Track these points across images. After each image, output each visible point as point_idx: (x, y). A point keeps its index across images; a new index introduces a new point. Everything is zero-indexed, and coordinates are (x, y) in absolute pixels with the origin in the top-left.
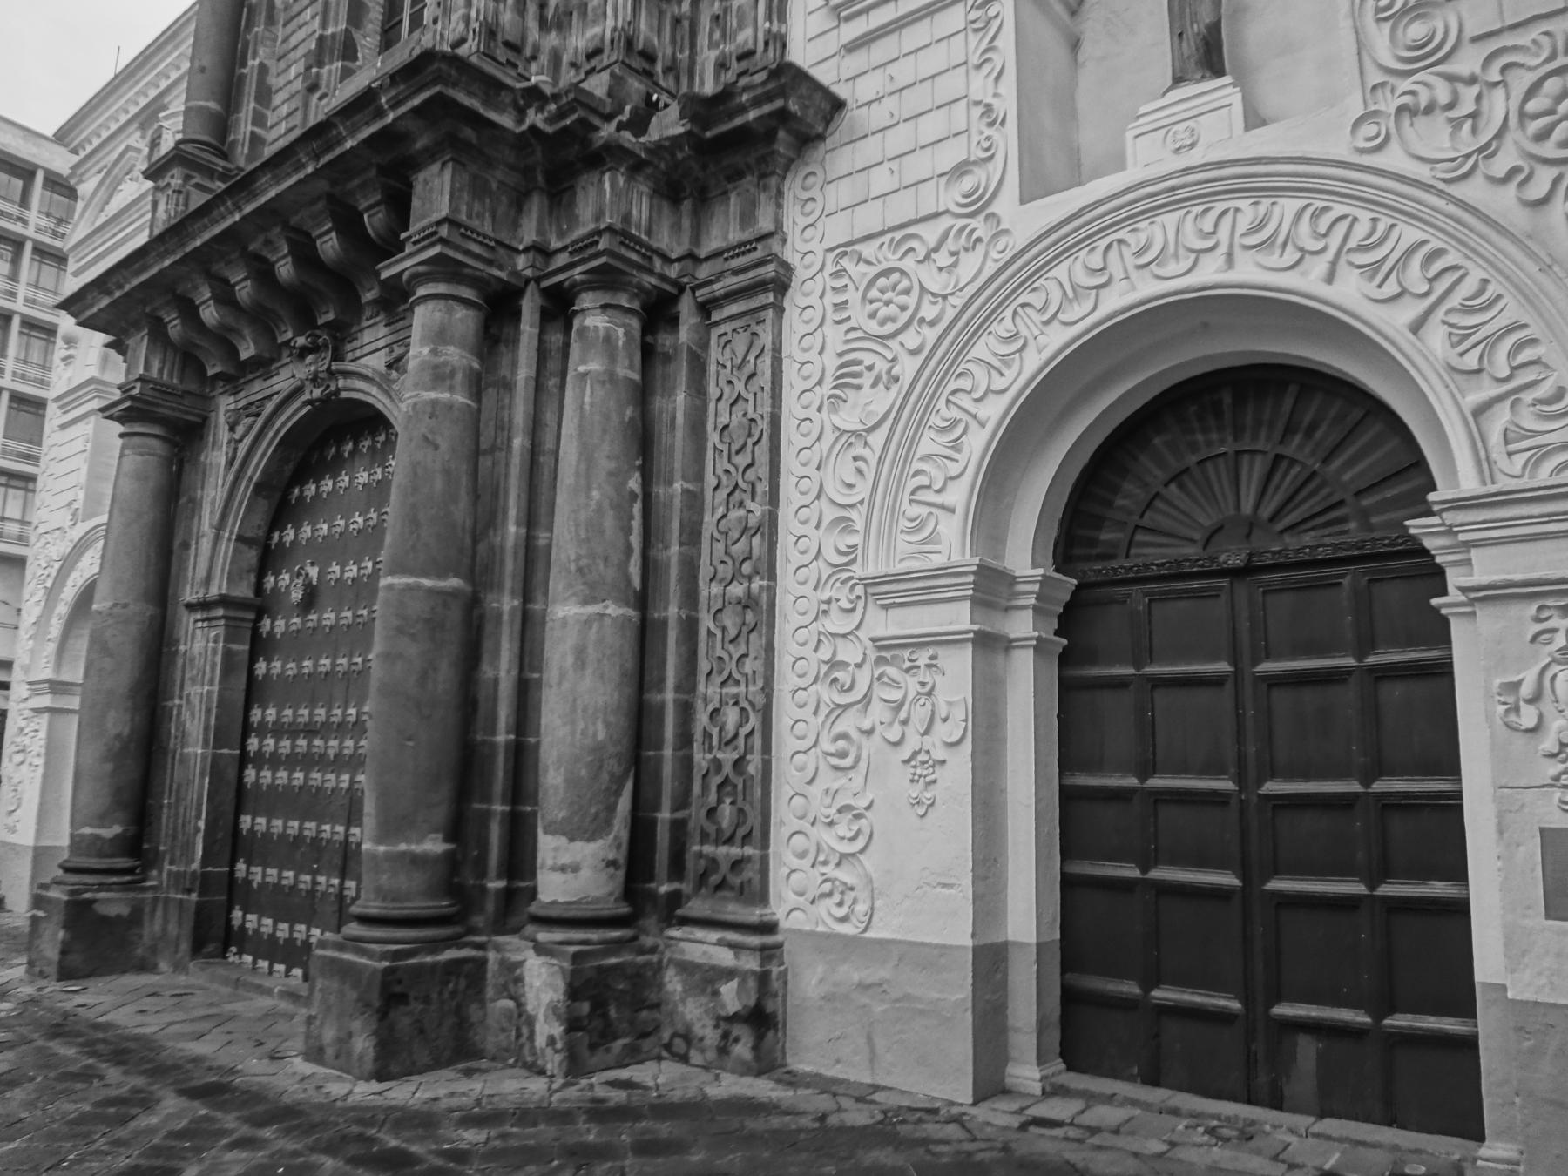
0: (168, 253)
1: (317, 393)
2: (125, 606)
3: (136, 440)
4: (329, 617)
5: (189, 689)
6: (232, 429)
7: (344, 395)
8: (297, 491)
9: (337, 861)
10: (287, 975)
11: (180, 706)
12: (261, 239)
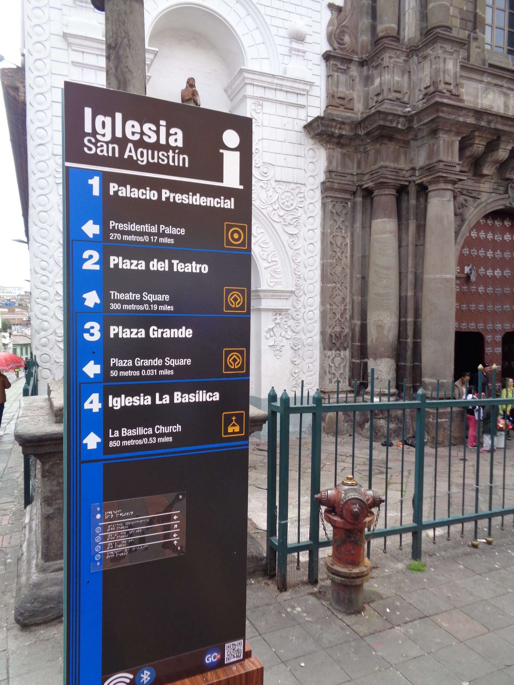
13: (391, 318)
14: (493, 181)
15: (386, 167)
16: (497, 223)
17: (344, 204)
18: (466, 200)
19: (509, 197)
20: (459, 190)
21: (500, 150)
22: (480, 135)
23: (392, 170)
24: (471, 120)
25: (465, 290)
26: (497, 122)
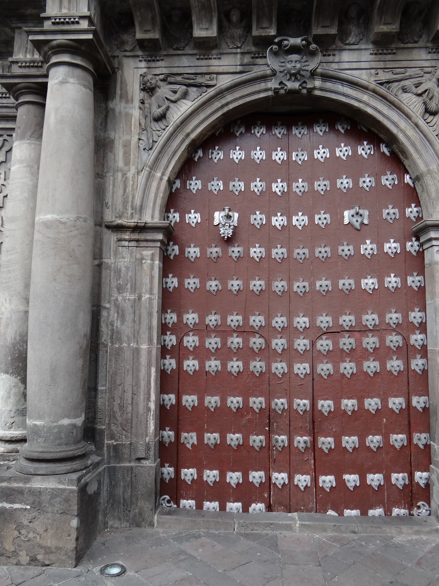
3: (78, 72)
4: (256, 252)
5: (115, 294)
6: (149, 89)
7: (317, 93)
8: (200, 153)
9: (308, 425)
10: (245, 509)
11: (109, 309)
13: (10, 303)
14: (239, 50)
15: (17, 62)
16: (295, 131)
17: (5, 137)
18: (175, 92)
20: (162, 77)
23: (28, 64)
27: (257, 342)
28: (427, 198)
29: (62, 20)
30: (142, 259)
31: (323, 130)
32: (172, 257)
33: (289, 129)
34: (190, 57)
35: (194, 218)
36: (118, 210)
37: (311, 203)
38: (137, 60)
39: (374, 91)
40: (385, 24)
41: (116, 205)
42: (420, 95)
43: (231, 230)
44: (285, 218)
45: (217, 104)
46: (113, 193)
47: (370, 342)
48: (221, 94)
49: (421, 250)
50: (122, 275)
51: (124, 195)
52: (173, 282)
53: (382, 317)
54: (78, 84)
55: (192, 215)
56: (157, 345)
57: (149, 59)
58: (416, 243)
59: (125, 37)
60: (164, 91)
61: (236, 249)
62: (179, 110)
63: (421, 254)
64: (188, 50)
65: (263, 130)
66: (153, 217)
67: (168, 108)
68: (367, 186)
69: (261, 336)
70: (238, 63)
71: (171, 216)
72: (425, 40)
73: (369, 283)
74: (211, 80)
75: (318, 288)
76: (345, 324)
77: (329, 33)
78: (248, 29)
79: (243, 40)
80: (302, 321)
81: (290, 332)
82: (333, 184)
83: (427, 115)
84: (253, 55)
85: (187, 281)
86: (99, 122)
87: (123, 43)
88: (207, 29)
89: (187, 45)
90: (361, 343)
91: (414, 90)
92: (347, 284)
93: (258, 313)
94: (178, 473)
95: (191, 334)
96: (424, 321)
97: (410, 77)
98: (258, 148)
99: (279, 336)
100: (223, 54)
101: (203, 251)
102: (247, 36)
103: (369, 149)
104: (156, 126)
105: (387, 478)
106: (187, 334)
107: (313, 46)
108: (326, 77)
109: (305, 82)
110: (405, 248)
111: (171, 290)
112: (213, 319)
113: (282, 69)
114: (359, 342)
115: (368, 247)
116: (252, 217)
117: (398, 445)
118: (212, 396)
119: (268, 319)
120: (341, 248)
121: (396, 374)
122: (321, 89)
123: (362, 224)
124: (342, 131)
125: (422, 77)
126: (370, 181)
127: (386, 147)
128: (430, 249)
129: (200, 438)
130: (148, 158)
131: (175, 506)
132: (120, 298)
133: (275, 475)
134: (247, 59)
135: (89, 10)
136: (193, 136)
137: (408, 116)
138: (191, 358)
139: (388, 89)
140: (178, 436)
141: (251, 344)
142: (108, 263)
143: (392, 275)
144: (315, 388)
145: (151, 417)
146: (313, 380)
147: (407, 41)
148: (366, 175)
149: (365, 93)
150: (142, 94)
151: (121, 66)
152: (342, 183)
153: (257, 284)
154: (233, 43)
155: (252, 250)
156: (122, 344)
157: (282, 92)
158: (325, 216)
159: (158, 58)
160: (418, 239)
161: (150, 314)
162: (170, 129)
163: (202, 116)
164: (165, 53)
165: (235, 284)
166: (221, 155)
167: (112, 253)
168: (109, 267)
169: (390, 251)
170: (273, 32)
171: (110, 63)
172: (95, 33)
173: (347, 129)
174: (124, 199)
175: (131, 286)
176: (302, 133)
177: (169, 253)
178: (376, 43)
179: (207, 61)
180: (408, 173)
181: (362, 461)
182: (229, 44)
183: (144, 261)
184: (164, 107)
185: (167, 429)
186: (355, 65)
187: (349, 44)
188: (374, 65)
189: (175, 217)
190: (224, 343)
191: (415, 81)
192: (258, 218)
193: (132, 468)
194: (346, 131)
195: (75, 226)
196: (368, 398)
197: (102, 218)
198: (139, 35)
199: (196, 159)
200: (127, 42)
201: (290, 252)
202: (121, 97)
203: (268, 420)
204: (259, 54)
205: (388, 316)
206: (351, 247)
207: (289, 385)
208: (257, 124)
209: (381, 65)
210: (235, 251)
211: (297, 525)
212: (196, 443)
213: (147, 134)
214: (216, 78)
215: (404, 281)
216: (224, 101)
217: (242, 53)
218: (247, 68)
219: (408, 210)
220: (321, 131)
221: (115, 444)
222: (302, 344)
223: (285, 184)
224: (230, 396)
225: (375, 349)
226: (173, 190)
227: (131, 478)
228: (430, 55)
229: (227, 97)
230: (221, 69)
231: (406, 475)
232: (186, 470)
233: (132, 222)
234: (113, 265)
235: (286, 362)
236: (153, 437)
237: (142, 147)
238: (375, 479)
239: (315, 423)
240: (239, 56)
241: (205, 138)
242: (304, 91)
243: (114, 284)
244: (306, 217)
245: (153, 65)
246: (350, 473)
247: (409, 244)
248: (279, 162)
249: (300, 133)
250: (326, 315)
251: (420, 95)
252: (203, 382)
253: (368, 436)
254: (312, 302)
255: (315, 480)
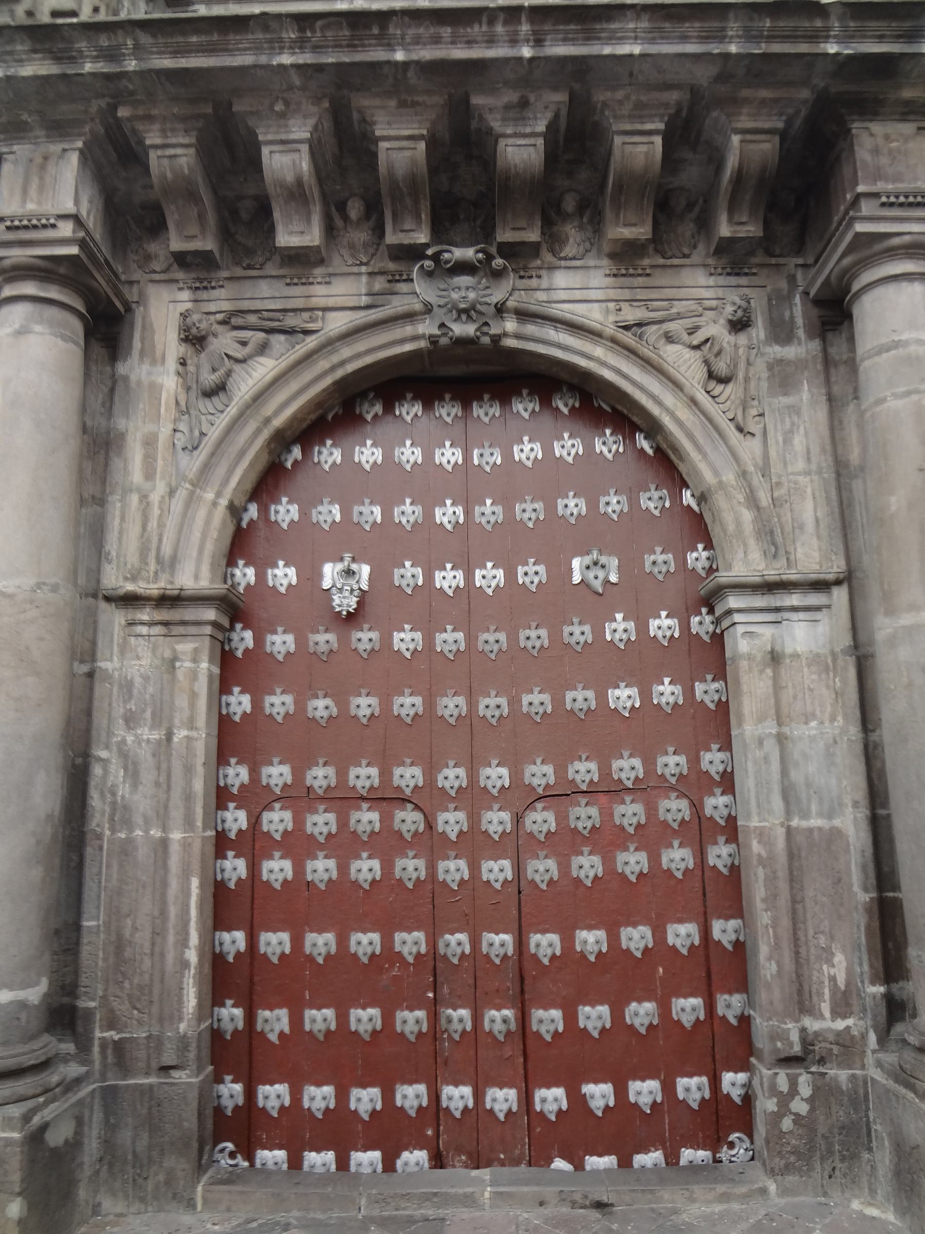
0: (300, 44)
1: (463, 329)
2: (55, 588)
4: (406, 639)
5: (120, 731)
6: (195, 339)
7: (510, 343)
8: (297, 452)
9: (510, 984)
10: (389, 1165)
12: (511, 96)
14: (364, 269)
16: (477, 411)
18: (244, 344)
19: (428, 309)
20: (220, 317)
21: (265, 151)
22: (140, 112)
24: (35, 67)
25: (323, 648)
26: (137, 47)
27: (408, 820)
28: (722, 534)
29: (25, 222)
30: (175, 659)
31: (530, 409)
32: (239, 654)
33: (466, 406)
34: (274, 281)
35: (284, 575)
36: (129, 566)
37: (508, 545)
38: (174, 286)
39: (614, 340)
40: (625, 225)
41: (125, 556)
42: (697, 347)
43: (355, 599)
44: (460, 574)
45: (323, 364)
46: (121, 533)
47: (630, 812)
48: (330, 344)
49: (718, 631)
50: (135, 692)
51: (142, 536)
52: (240, 703)
53: (649, 762)
54: (51, 334)
55: (279, 572)
56: (204, 830)
57: (198, 285)
58: (708, 619)
59: (153, 247)
60: (225, 342)
61: (365, 635)
62: (250, 376)
63: (718, 639)
64: (270, 269)
65: (417, 408)
66: (197, 577)
67: (229, 374)
68: (614, 512)
69: (417, 807)
70: (364, 291)
71: (238, 572)
72: (703, 253)
73: (623, 696)
74: (312, 320)
75: (525, 709)
76: (578, 778)
77: (527, 240)
78: (379, 231)
79: (371, 250)
80: (496, 775)
81: (473, 797)
82: (551, 508)
83: (712, 384)
84: (390, 278)
85: (269, 699)
86: (100, 401)
87: (148, 258)
88: (302, 233)
89: (268, 259)
90: (612, 815)
91: (685, 337)
92: (580, 698)
93: (408, 761)
94: (250, 1094)
95: (277, 805)
96: (729, 770)
97: (679, 316)
98: (408, 443)
99: (452, 806)
100: (335, 275)
101: (301, 642)
102: (379, 245)
103: (615, 442)
104: (206, 405)
105: (669, 1088)
106: (268, 807)
107: (498, 262)
108: (524, 315)
109: (486, 324)
110: (689, 629)
111: (237, 718)
112: (320, 776)
113: (442, 302)
114: (607, 814)
115: (619, 628)
116: (397, 572)
117: (687, 1020)
118: (320, 931)
119: (430, 773)
120: (567, 629)
121: (679, 875)
122: (518, 336)
123: (607, 582)
124: (565, 411)
125: (701, 316)
126: (618, 502)
127: (645, 438)
128: (731, 629)
129: (296, 1020)
130: (192, 464)
131: (246, 1164)
132: (130, 739)
133: (448, 1091)
134: (379, 284)
135: (77, 202)
136: (278, 422)
137: (677, 385)
138: (277, 854)
139: (640, 337)
140: (250, 1018)
141: (397, 825)
142: (107, 670)
143: (667, 680)
144: (523, 909)
145: (191, 981)
146: (520, 892)
147: (669, 254)
148: (612, 491)
149: (596, 343)
150: (183, 349)
151: (142, 300)
152: (566, 506)
153: (408, 704)
154: (353, 256)
155: (397, 636)
156: (131, 831)
157: (444, 341)
158: (537, 568)
159: (213, 284)
160: (711, 611)
161: (189, 770)
162: (232, 411)
163: (294, 385)
164: (225, 274)
165: (364, 705)
166: (337, 455)
167: (116, 649)
168: (107, 677)
169: (660, 634)
170: (422, 237)
171: (119, 294)
172: (82, 244)
173: (573, 406)
174: (143, 543)
175: (153, 714)
176: (491, 414)
177: (233, 645)
178: (612, 256)
179: (305, 287)
180: (688, 487)
181: (620, 1055)
182: (346, 257)
183: (178, 664)
184: (222, 372)
185: (229, 1002)
186: (578, 295)
187: (565, 259)
188: (612, 294)
189: (245, 575)
190: (343, 823)
191: (689, 323)
192: (409, 574)
193: (151, 1086)
194: (573, 410)
195: (32, 601)
196: (627, 925)
197: (98, 581)
198: (176, 244)
199: (289, 465)
200: (156, 256)
201: (470, 639)
202: (142, 353)
203: (433, 978)
204: (401, 275)
205: (661, 760)
206: (587, 628)
207: (474, 906)
208: (405, 398)
209: (627, 294)
210: (365, 638)
211: (487, 1195)
212: (287, 1030)
213: (190, 423)
214: (323, 318)
215: (689, 692)
216: (335, 359)
217: (370, 274)
218: (380, 299)
219: (691, 557)
220: (526, 410)
221: (116, 1038)
222: (496, 820)
223: (461, 508)
224: (356, 930)
225: (639, 826)
226: (244, 524)
227: (150, 1108)
228: (712, 278)
229: (342, 351)
230: (331, 302)
231: (704, 1079)
232: (268, 1087)
233: (152, 588)
234: (116, 673)
235: (467, 857)
236: (194, 1023)
237: (179, 444)
238: (644, 1091)
239: (523, 981)
240: (364, 279)
241: (304, 425)
242: (486, 340)
243: (119, 711)
244: (501, 571)
245: (204, 295)
246: (596, 1082)
247: (695, 620)
248: (449, 468)
249: (487, 414)
250: (543, 762)
251: (697, 347)
252: (300, 906)
253: (628, 1003)
254: (515, 738)
255: (527, 1099)
